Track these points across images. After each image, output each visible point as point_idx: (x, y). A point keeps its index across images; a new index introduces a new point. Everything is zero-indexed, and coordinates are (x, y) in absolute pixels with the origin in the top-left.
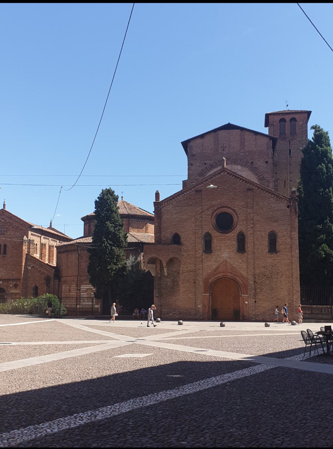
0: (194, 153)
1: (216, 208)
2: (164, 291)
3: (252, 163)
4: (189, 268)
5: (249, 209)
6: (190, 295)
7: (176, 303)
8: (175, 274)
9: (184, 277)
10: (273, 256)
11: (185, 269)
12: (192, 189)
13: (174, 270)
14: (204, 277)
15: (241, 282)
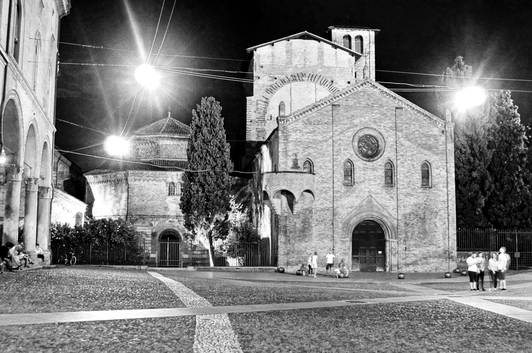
0: (262, 64)
1: (358, 129)
2: (291, 235)
3: (332, 82)
4: (325, 205)
5: (398, 132)
6: (326, 241)
8: (306, 213)
10: (426, 191)
11: (320, 206)
12: (328, 102)
13: (305, 207)
15: (389, 224)
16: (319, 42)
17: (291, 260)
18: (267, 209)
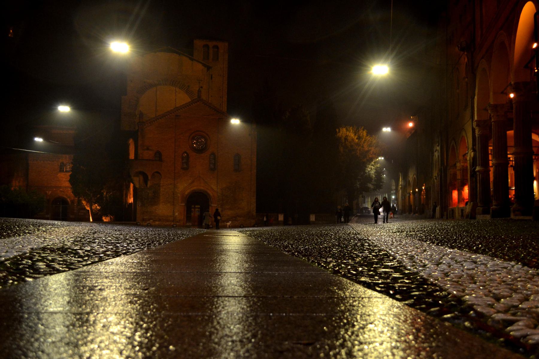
3: (189, 86)
7: (157, 211)
9: (164, 190)
14: (181, 190)
15: (211, 194)
16: (180, 55)
17: (145, 217)
18: (132, 185)
